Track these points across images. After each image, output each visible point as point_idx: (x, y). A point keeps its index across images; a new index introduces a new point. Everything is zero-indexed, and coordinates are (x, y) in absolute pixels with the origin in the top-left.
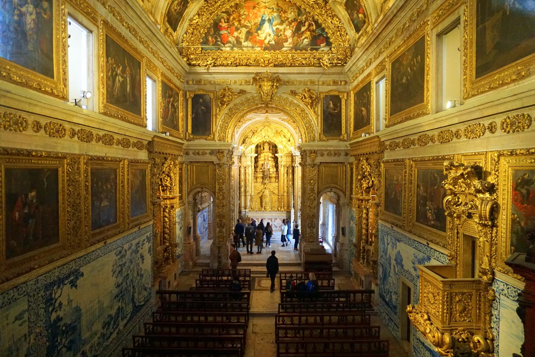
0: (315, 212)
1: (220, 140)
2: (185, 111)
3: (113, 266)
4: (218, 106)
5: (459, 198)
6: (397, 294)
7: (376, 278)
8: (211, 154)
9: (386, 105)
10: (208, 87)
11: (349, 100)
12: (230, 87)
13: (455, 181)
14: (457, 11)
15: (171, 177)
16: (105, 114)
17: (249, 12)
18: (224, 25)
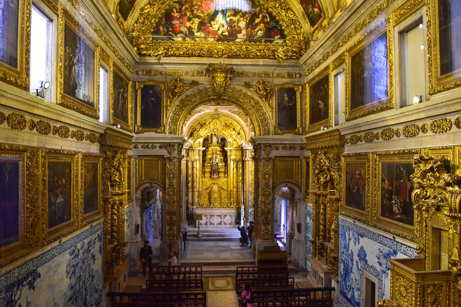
0: (270, 208)
1: (170, 133)
2: (134, 102)
3: (67, 266)
4: (169, 97)
5: (427, 192)
6: (360, 290)
7: (337, 275)
8: (160, 147)
9: (346, 99)
10: (159, 78)
11: (304, 93)
12: (181, 77)
13: (424, 175)
14: (418, 11)
15: (119, 171)
16: (62, 105)
17: (201, 3)
18: (176, 15)
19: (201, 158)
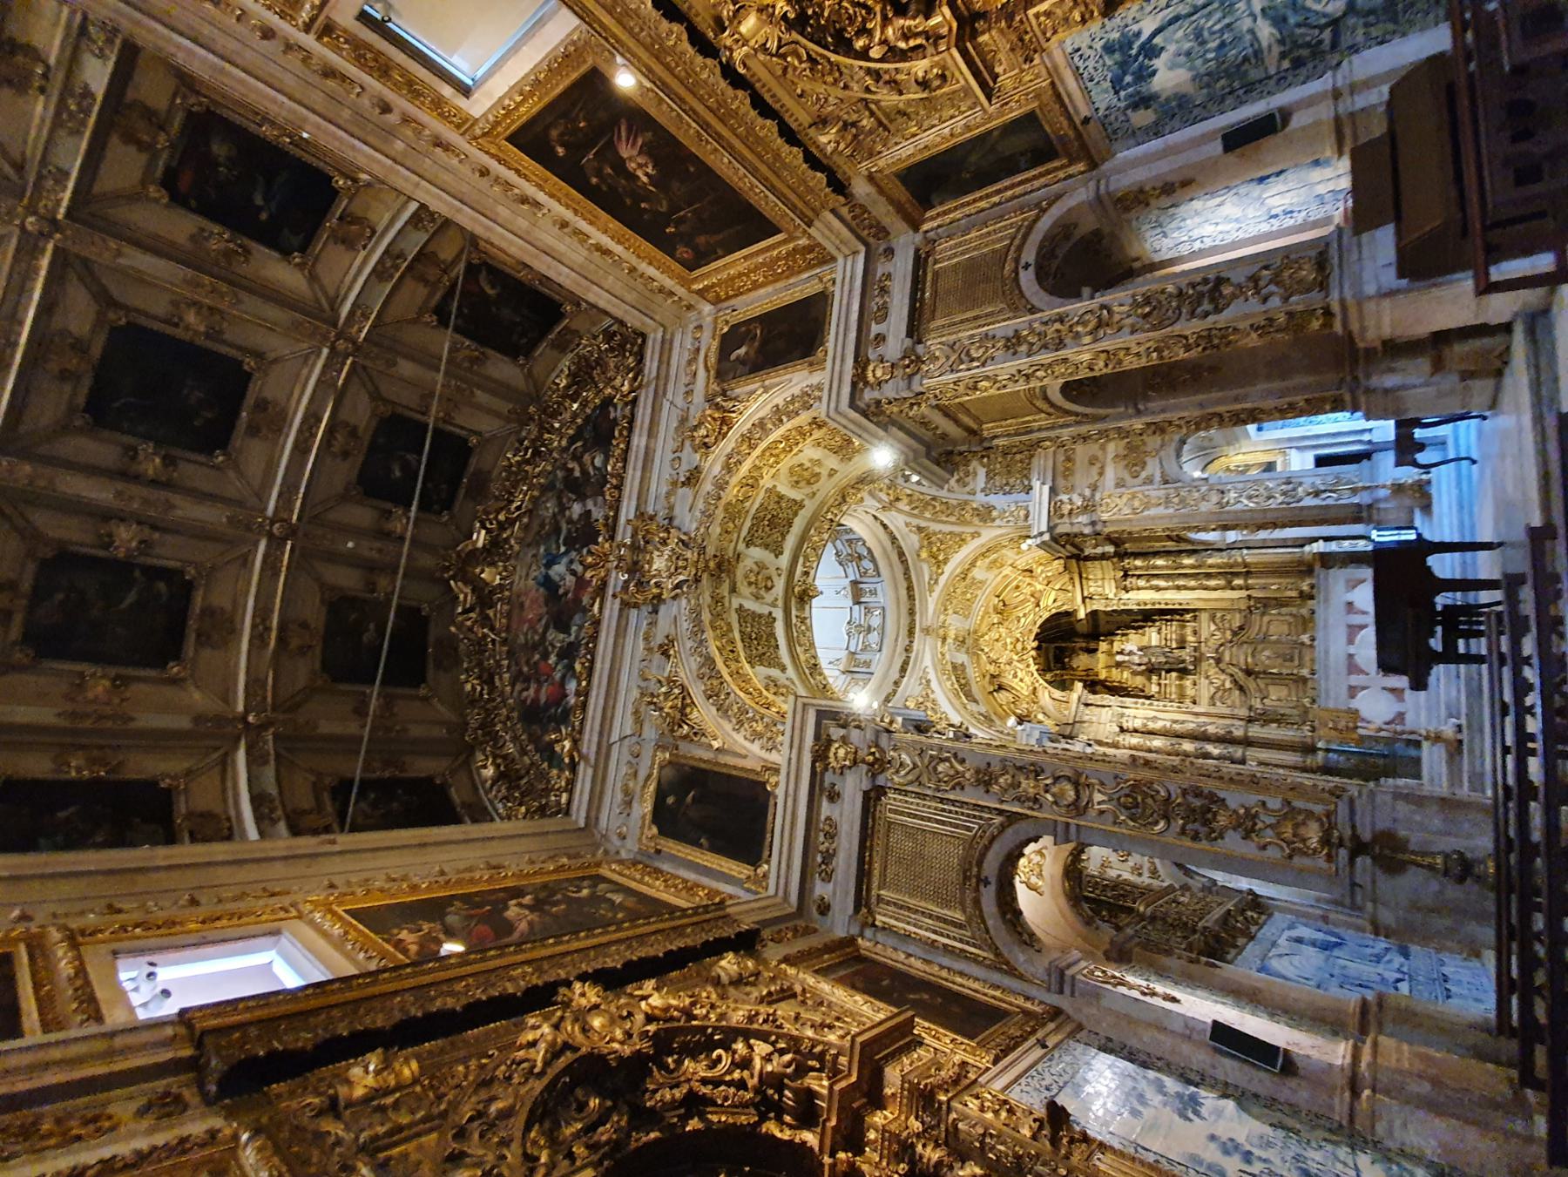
8: (834, 797)
19: (1113, 700)
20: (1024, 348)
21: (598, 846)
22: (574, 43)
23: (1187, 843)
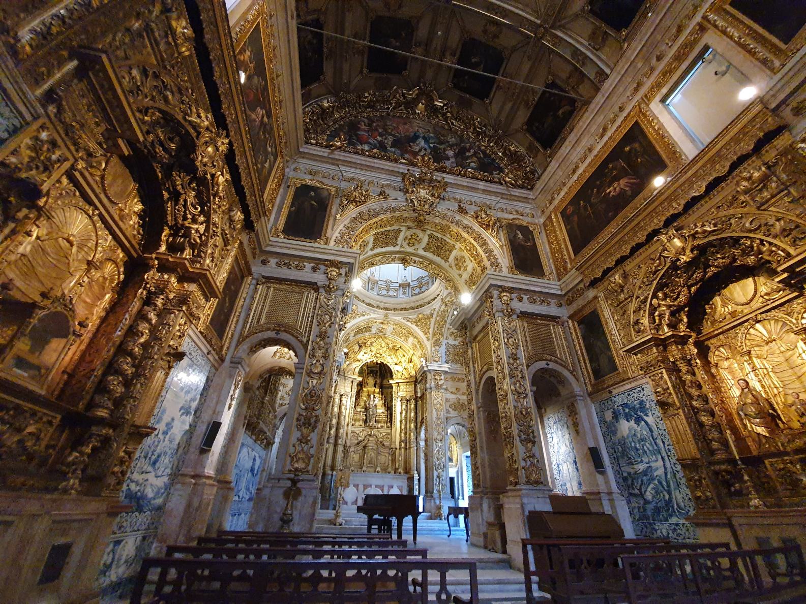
8: (315, 269)
19: (354, 393)
20: (511, 361)
21: (291, 157)
22: (680, 156)
23: (296, 416)
